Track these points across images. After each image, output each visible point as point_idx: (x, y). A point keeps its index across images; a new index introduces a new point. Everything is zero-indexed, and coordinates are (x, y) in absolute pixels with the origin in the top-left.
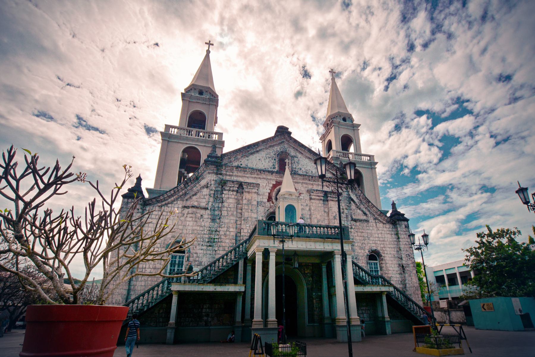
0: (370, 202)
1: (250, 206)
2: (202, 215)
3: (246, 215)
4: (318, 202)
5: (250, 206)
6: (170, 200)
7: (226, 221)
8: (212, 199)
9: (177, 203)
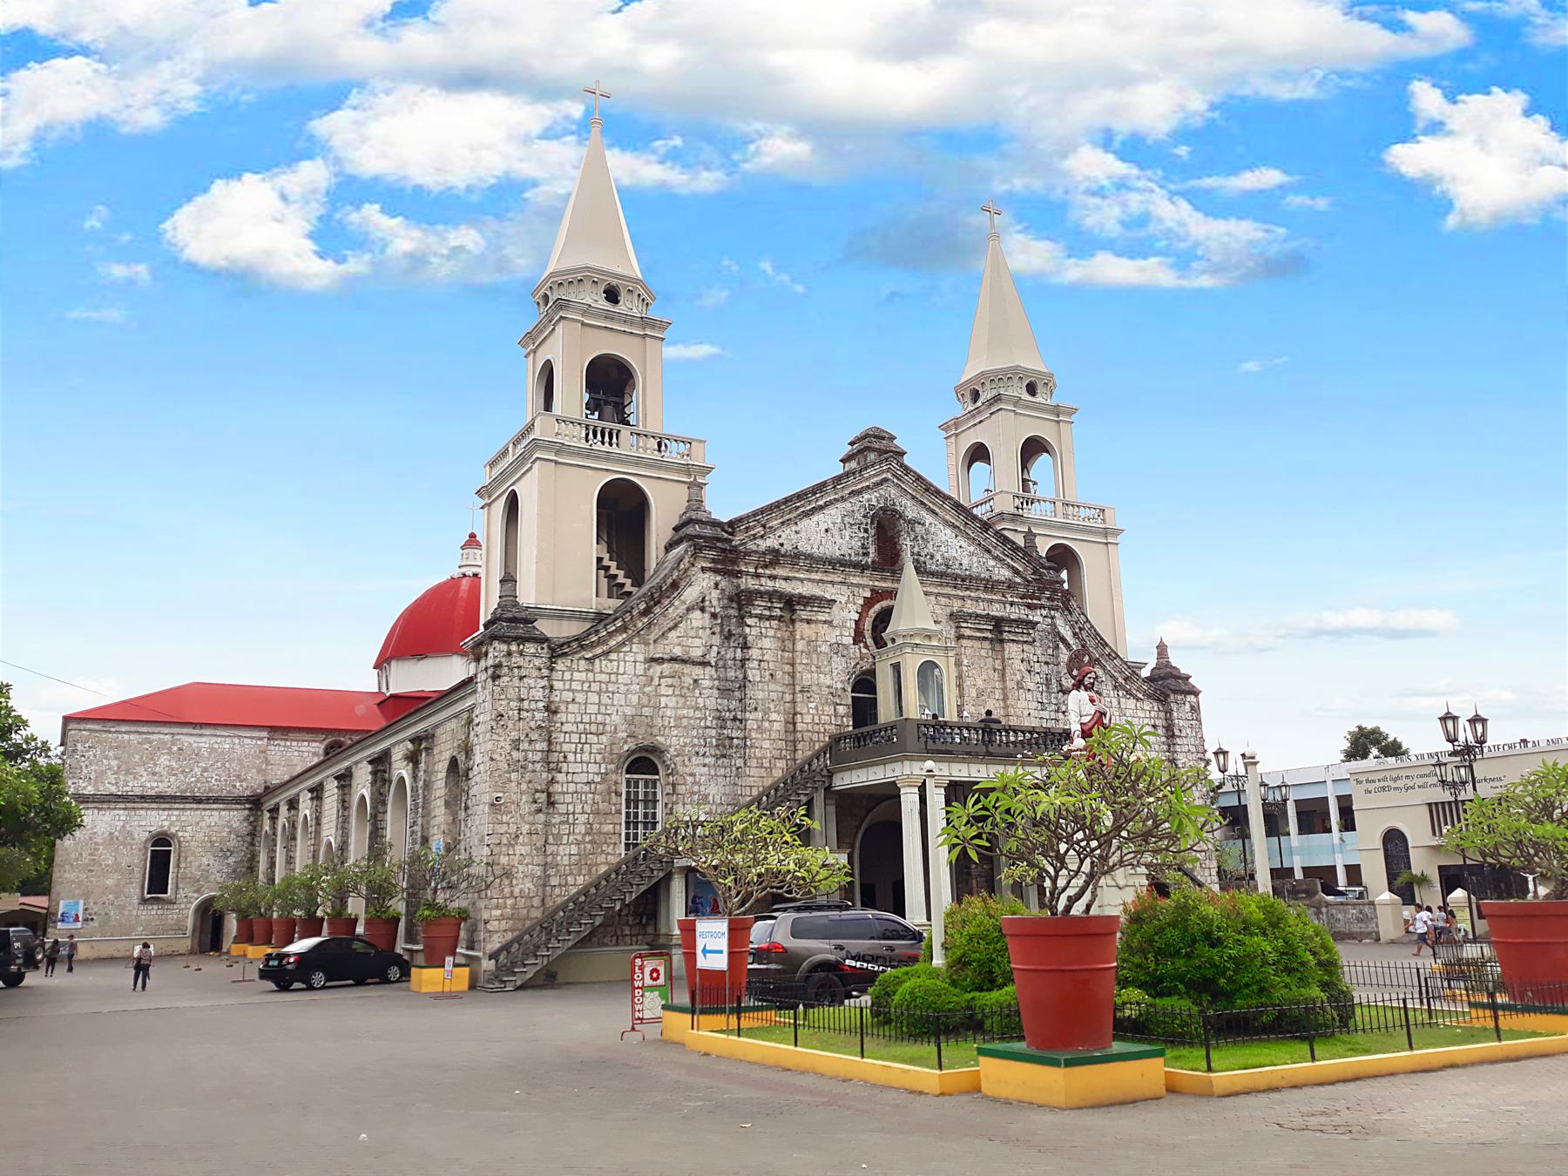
0: (1107, 645)
1: (814, 656)
2: (696, 681)
3: (806, 678)
4: (977, 644)
5: (814, 656)
6: (612, 643)
7: (760, 695)
8: (716, 640)
9: (630, 651)
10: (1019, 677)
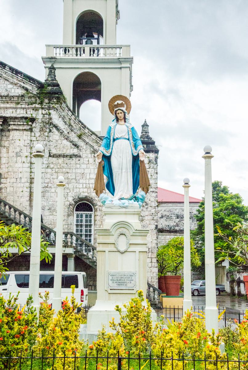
10: (18, 150)
